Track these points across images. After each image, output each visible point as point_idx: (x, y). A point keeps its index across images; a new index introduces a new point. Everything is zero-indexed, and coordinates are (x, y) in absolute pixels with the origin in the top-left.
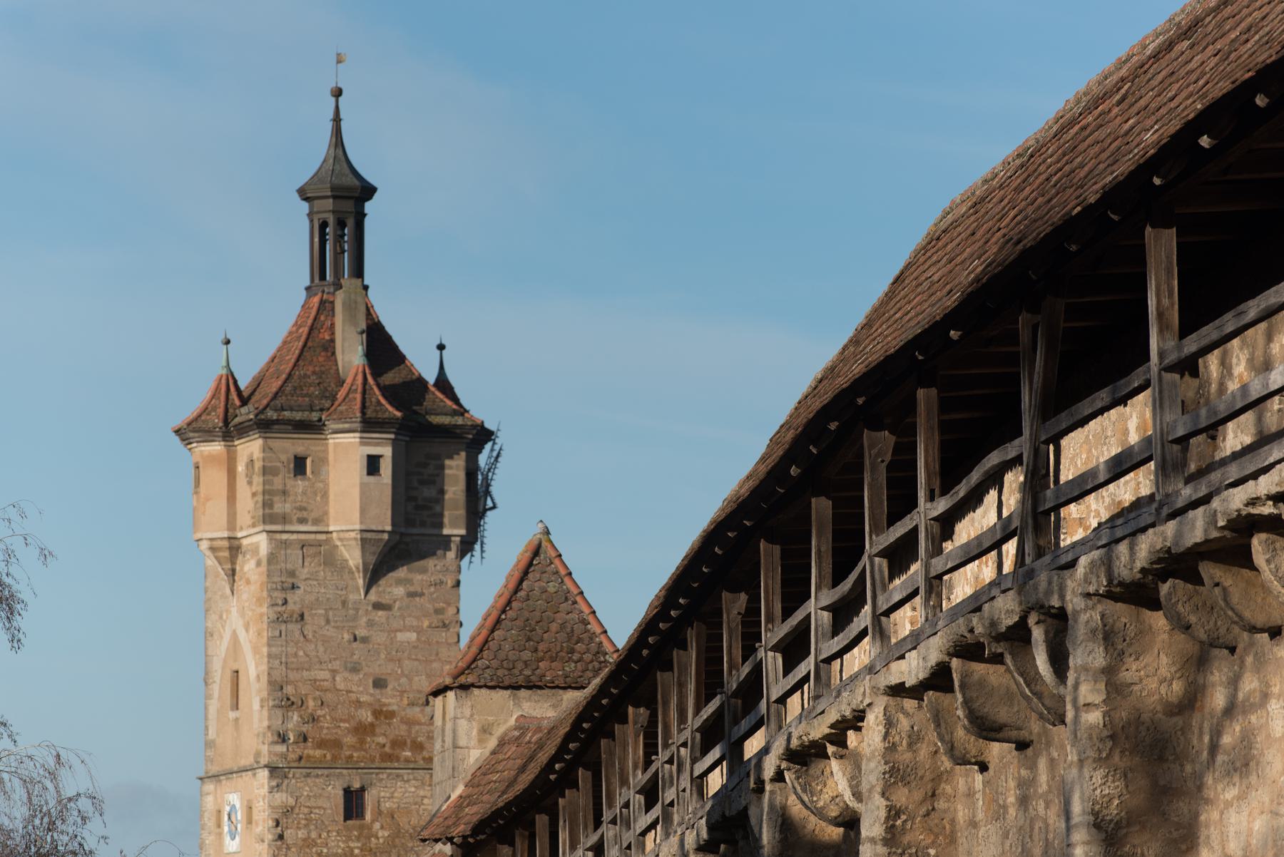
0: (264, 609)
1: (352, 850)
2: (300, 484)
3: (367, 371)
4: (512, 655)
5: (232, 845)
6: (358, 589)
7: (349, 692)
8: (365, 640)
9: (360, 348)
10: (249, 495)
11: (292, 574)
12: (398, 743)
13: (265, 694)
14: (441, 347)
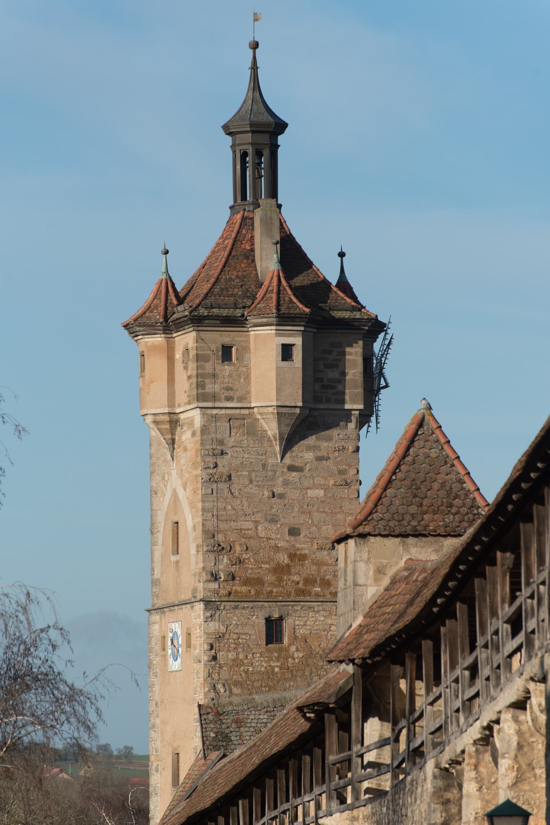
0: (199, 472)
1: (273, 668)
2: (227, 369)
3: (281, 275)
4: (401, 509)
5: (175, 665)
6: (275, 454)
7: (268, 539)
8: (282, 496)
9: (275, 256)
10: (186, 378)
11: (221, 442)
12: (310, 581)
13: (200, 541)
14: (342, 255)
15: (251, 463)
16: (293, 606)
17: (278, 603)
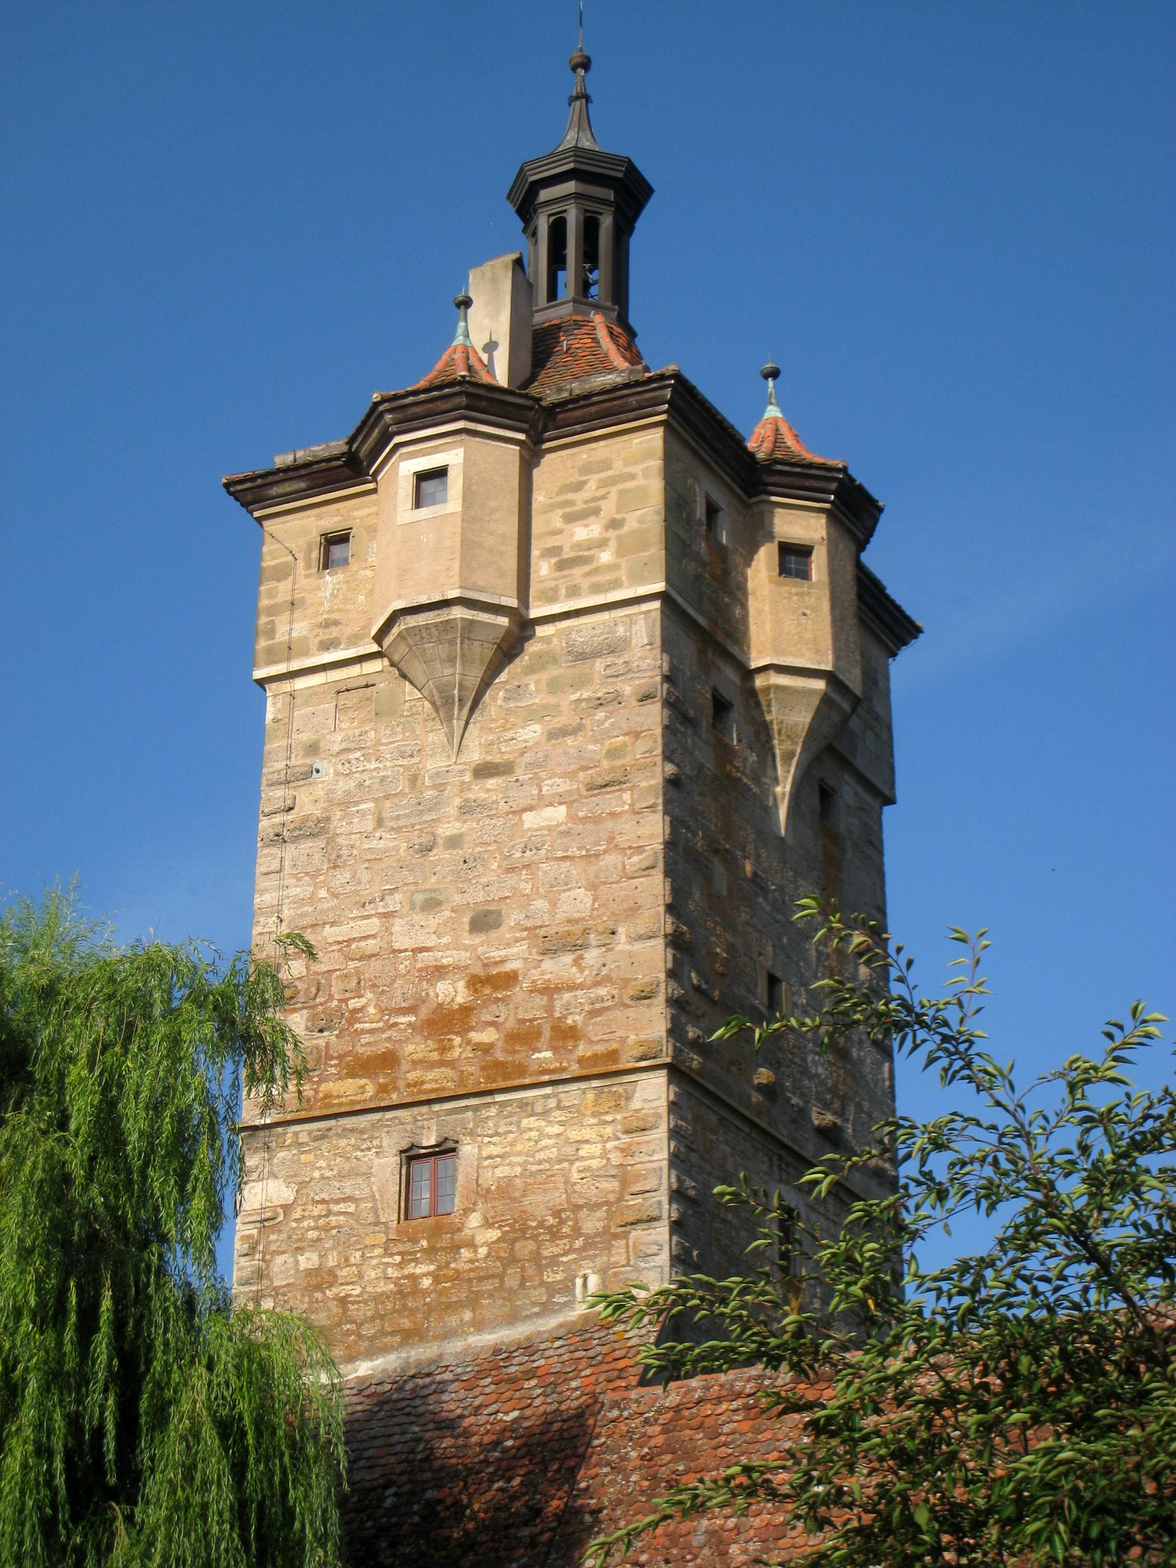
8: (454, 842)
15: (383, 779)
16: (476, 1109)
17: (436, 1107)
